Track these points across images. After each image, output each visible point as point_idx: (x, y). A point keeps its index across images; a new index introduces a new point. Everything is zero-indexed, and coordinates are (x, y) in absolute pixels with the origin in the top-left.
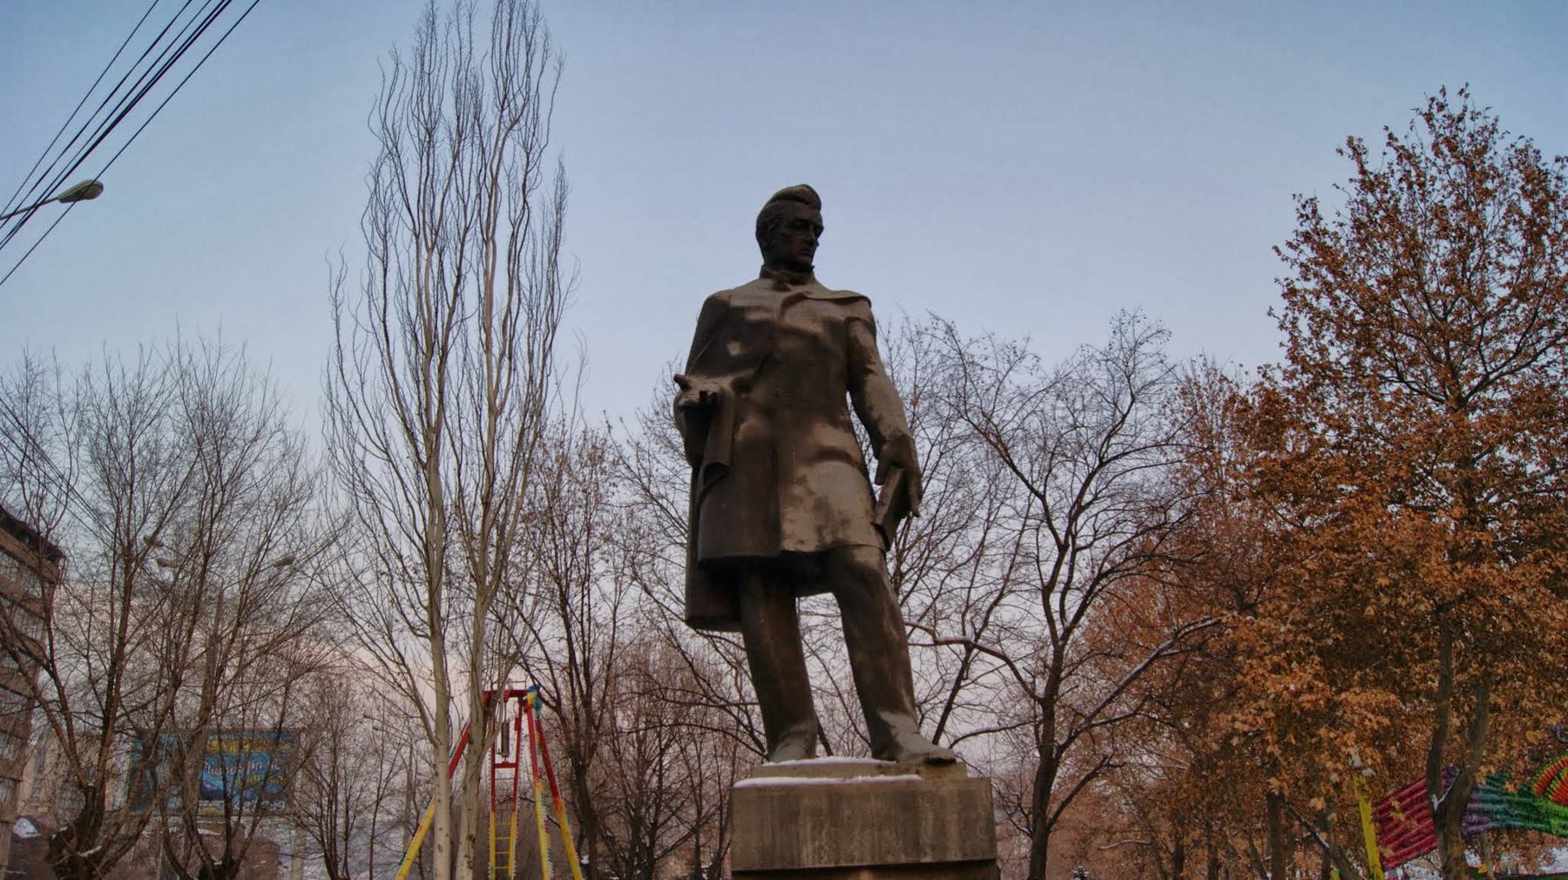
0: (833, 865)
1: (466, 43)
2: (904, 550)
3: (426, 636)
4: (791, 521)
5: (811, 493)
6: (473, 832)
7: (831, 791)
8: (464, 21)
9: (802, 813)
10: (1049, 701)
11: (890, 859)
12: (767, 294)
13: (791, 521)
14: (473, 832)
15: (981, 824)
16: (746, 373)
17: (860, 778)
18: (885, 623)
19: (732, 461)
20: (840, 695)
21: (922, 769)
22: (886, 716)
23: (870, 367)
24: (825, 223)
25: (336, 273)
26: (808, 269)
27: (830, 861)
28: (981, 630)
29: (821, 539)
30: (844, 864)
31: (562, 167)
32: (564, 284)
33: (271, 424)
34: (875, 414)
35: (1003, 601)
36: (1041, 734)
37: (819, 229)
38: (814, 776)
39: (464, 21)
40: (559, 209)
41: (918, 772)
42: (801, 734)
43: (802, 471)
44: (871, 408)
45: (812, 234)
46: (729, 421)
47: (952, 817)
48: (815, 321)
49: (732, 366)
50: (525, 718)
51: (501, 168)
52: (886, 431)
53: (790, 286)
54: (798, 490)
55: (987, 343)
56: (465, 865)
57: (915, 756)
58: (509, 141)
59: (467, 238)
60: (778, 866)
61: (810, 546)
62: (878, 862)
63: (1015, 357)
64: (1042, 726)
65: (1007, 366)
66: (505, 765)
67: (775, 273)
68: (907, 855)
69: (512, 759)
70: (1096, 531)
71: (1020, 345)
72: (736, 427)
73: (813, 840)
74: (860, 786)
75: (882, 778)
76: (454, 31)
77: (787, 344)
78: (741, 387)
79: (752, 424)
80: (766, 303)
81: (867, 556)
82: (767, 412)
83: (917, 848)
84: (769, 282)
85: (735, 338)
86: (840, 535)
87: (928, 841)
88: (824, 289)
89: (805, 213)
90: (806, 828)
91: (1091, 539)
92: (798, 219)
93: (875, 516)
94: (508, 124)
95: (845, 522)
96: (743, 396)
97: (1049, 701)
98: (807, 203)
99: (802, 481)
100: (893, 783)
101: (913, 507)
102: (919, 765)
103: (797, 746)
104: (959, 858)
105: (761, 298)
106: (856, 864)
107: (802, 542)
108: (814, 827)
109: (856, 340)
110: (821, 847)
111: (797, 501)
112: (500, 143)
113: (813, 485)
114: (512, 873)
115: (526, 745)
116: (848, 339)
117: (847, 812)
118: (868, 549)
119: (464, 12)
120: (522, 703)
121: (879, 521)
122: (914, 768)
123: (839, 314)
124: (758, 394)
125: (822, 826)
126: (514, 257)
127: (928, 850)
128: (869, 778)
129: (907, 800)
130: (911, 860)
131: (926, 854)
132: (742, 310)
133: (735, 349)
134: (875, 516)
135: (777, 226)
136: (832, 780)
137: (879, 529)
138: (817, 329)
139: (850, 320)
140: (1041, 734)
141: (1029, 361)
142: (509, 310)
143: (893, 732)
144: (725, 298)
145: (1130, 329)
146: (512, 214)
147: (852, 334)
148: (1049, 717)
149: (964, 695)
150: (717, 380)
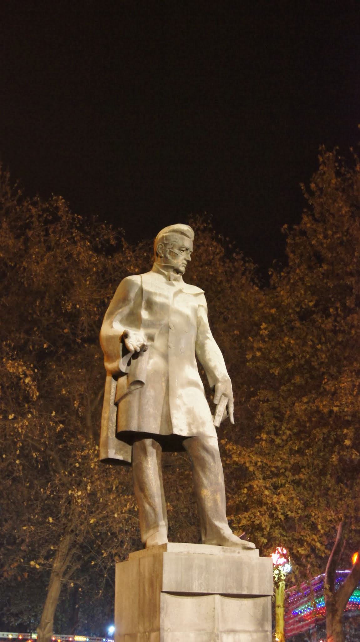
5: (185, 404)
11: (230, 592)
13: (176, 418)
19: (146, 381)
27: (205, 590)
29: (190, 430)
43: (180, 391)
47: (256, 575)
61: (184, 433)
62: (225, 592)
67: (166, 273)
68: (237, 590)
72: (148, 363)
73: (198, 581)
77: (175, 320)
80: (166, 293)
82: (165, 357)
86: (201, 430)
99: (180, 397)
107: (181, 430)
110: (201, 583)
116: (198, 318)
118: (213, 438)
124: (159, 343)
127: (245, 588)
131: (244, 591)
143: (222, 532)
147: (199, 315)
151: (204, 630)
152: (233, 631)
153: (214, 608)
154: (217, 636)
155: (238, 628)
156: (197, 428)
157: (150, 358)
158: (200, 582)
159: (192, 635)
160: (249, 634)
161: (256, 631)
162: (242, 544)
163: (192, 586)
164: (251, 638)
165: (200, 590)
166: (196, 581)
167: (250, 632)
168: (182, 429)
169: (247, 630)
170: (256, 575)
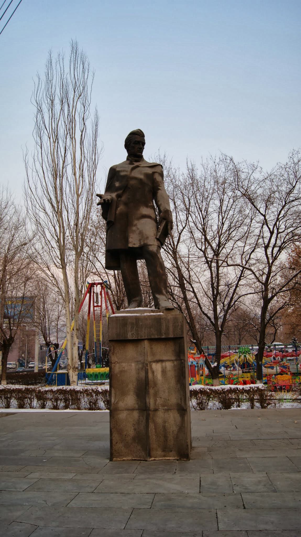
0: (136, 338)
1: (62, 69)
2: (221, 234)
3: (61, 268)
4: (132, 238)
5: (138, 229)
6: (78, 328)
7: (136, 318)
8: (61, 60)
9: (128, 323)
10: (266, 284)
11: (153, 337)
12: (127, 166)
13: (132, 238)
14: (78, 328)
15: (179, 327)
16: (120, 192)
17: (146, 314)
18: (158, 268)
20: (200, 283)
21: (164, 311)
22: (158, 296)
23: (160, 188)
24: (146, 142)
25: (25, 152)
26: (142, 157)
27: (135, 337)
28: (248, 260)
29: (140, 243)
30: (139, 338)
31: (96, 110)
32: (99, 151)
33: (10, 203)
34: (159, 203)
35: (256, 250)
36: (264, 294)
37: (144, 144)
38: (133, 313)
39: (61, 60)
40: (97, 125)
41: (163, 312)
42: (136, 301)
43: (136, 222)
44: (159, 201)
45: (142, 146)
46: (114, 207)
47: (171, 325)
48: (141, 174)
49: (117, 189)
50: (103, 290)
51: (76, 112)
52: (162, 209)
53: (134, 163)
54: (134, 228)
55: (244, 163)
56: (76, 337)
57: (163, 307)
58: (79, 103)
59: (67, 137)
60: (121, 339)
61: (137, 245)
62: (149, 337)
63: (254, 168)
64: (264, 293)
65: (252, 171)
66: (98, 306)
68: (158, 336)
69: (100, 304)
70: (286, 227)
71: (256, 164)
73: (131, 332)
74: (145, 316)
75: (152, 314)
76: (58, 65)
77: (132, 182)
78: (119, 196)
79: (121, 208)
80: (126, 169)
81: (153, 248)
82: (126, 204)
83: (161, 334)
84: (128, 162)
85: (117, 181)
86: (145, 242)
87: (163, 331)
88: (147, 162)
89: (138, 139)
90: (129, 328)
91: (284, 229)
92: (136, 141)
93: (157, 236)
94: (78, 96)
95: (147, 238)
96: (119, 199)
97: (266, 284)
98: (139, 135)
100: (154, 315)
101: (169, 232)
102: (164, 310)
103: (134, 304)
104: (172, 337)
105: (126, 167)
106: (143, 338)
107: (134, 244)
108: (131, 328)
109: (155, 179)
110: (133, 333)
111: (133, 232)
112: (75, 104)
113: (139, 226)
114: (101, 339)
115: (103, 299)
117: (141, 324)
118: (152, 246)
119: (61, 57)
120: (102, 287)
121: (158, 237)
122: (162, 311)
123: (150, 171)
124: (124, 198)
125: (133, 328)
126: (82, 142)
127: (164, 334)
128: (148, 314)
129: (158, 320)
130: (159, 337)
131: (163, 336)
132: (119, 172)
133: (117, 184)
134: (157, 236)
135: (130, 144)
136: (138, 315)
137: (158, 239)
138: (142, 177)
139: (154, 173)
140: (264, 294)
141: (259, 169)
142: (81, 160)
143: (159, 301)
144: (115, 168)
145: (297, 156)
146: (81, 128)
147: (154, 177)
148: (266, 290)
149: (241, 282)
150: (111, 194)
151: (140, 361)
152: (162, 361)
153: (144, 348)
154: (147, 365)
155: (165, 358)
156: (144, 241)
157: (117, 207)
158: (132, 332)
159: (133, 364)
160: (172, 362)
161: (176, 360)
162: (165, 307)
163: (127, 336)
164: (173, 365)
165: (133, 337)
166: (130, 333)
167: (172, 360)
168: (135, 243)
169: (171, 359)
170: (171, 325)
